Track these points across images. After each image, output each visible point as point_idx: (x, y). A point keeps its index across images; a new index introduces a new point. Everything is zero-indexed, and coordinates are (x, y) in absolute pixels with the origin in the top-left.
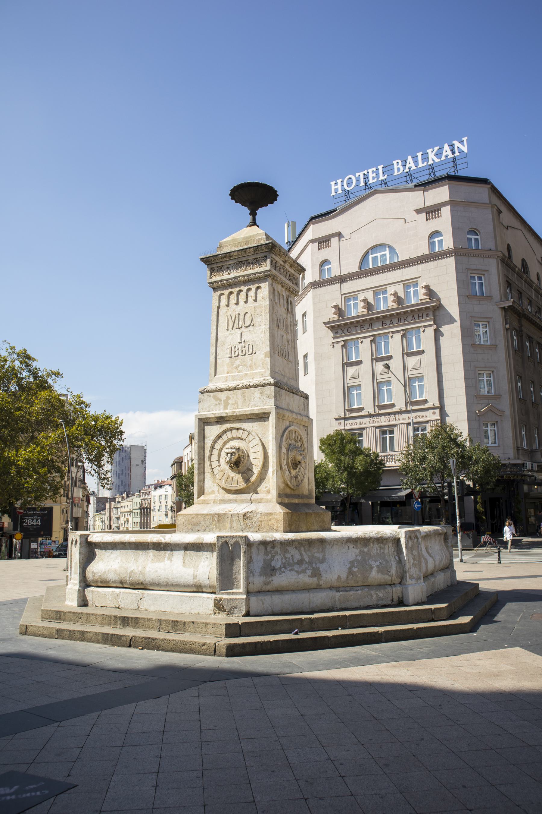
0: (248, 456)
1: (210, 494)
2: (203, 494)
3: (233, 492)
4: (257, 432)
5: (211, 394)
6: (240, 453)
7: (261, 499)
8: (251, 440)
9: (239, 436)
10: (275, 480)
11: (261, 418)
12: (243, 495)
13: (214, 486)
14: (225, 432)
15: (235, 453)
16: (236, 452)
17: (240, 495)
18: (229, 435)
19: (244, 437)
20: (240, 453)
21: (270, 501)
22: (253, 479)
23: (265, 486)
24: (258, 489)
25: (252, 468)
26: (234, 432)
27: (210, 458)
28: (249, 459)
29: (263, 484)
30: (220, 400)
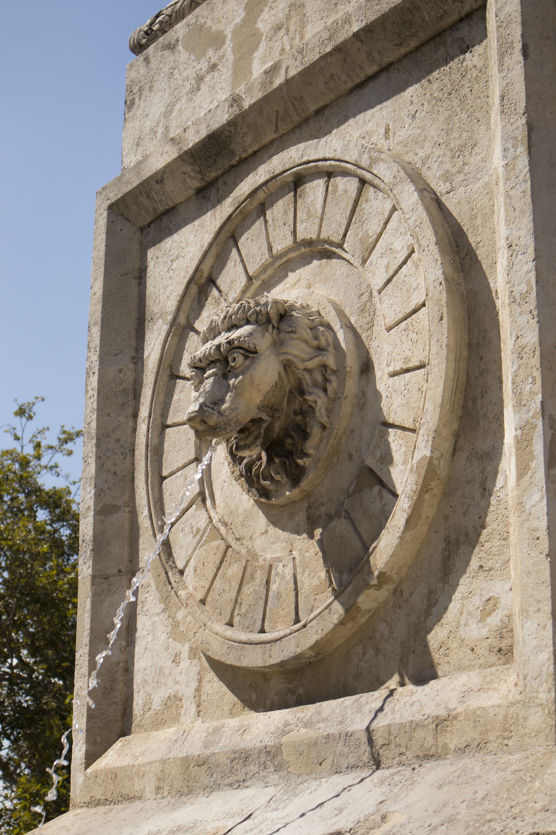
0: (367, 368)
1: (159, 723)
2: (125, 732)
3: (277, 684)
4: (415, 157)
5: (180, 30)
6: (297, 350)
7: (441, 723)
8: (374, 227)
9: (307, 230)
10: (542, 523)
11: (437, 37)
12: (329, 707)
13: (176, 660)
14: (228, 238)
15: (250, 353)
16: (263, 343)
17: (309, 710)
18: (253, 247)
19: (332, 231)
20: (297, 350)
21: (506, 732)
22: (386, 549)
23: (477, 602)
24: (436, 637)
25: (387, 458)
26: (279, 211)
27: (157, 452)
28: (368, 398)
29: (465, 585)
30: (217, 40)
